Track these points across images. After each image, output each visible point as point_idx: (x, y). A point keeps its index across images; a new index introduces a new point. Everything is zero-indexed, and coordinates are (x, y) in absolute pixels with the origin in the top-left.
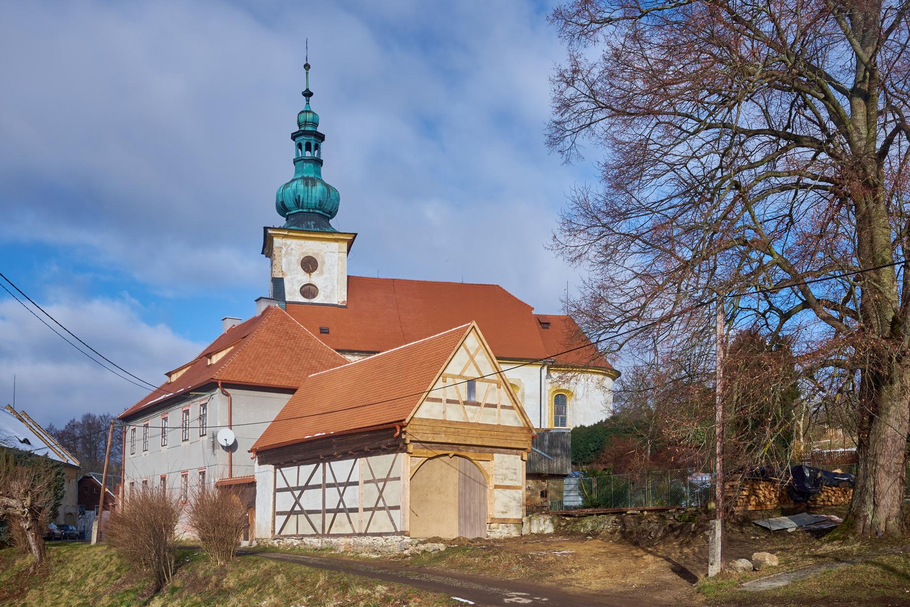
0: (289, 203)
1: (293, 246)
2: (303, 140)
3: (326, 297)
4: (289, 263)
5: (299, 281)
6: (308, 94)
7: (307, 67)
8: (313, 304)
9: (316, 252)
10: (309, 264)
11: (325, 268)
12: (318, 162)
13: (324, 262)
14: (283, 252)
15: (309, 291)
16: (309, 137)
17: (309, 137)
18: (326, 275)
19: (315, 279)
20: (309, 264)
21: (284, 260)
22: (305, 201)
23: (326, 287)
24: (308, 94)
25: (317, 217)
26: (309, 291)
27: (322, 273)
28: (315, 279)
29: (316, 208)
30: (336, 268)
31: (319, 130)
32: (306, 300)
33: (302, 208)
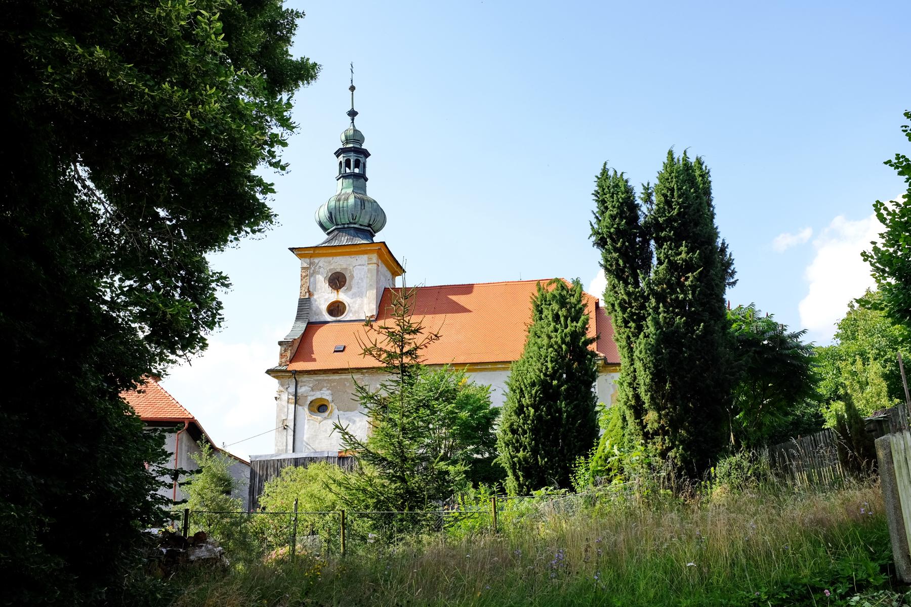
1: (321, 264)
2: (341, 158)
5: (326, 300)
6: (353, 114)
8: (340, 321)
9: (344, 266)
10: (337, 281)
11: (354, 282)
12: (362, 177)
13: (352, 277)
15: (336, 309)
19: (342, 296)
22: (338, 217)
24: (353, 114)
25: (352, 232)
27: (350, 289)
28: (342, 296)
29: (351, 223)
31: (364, 146)
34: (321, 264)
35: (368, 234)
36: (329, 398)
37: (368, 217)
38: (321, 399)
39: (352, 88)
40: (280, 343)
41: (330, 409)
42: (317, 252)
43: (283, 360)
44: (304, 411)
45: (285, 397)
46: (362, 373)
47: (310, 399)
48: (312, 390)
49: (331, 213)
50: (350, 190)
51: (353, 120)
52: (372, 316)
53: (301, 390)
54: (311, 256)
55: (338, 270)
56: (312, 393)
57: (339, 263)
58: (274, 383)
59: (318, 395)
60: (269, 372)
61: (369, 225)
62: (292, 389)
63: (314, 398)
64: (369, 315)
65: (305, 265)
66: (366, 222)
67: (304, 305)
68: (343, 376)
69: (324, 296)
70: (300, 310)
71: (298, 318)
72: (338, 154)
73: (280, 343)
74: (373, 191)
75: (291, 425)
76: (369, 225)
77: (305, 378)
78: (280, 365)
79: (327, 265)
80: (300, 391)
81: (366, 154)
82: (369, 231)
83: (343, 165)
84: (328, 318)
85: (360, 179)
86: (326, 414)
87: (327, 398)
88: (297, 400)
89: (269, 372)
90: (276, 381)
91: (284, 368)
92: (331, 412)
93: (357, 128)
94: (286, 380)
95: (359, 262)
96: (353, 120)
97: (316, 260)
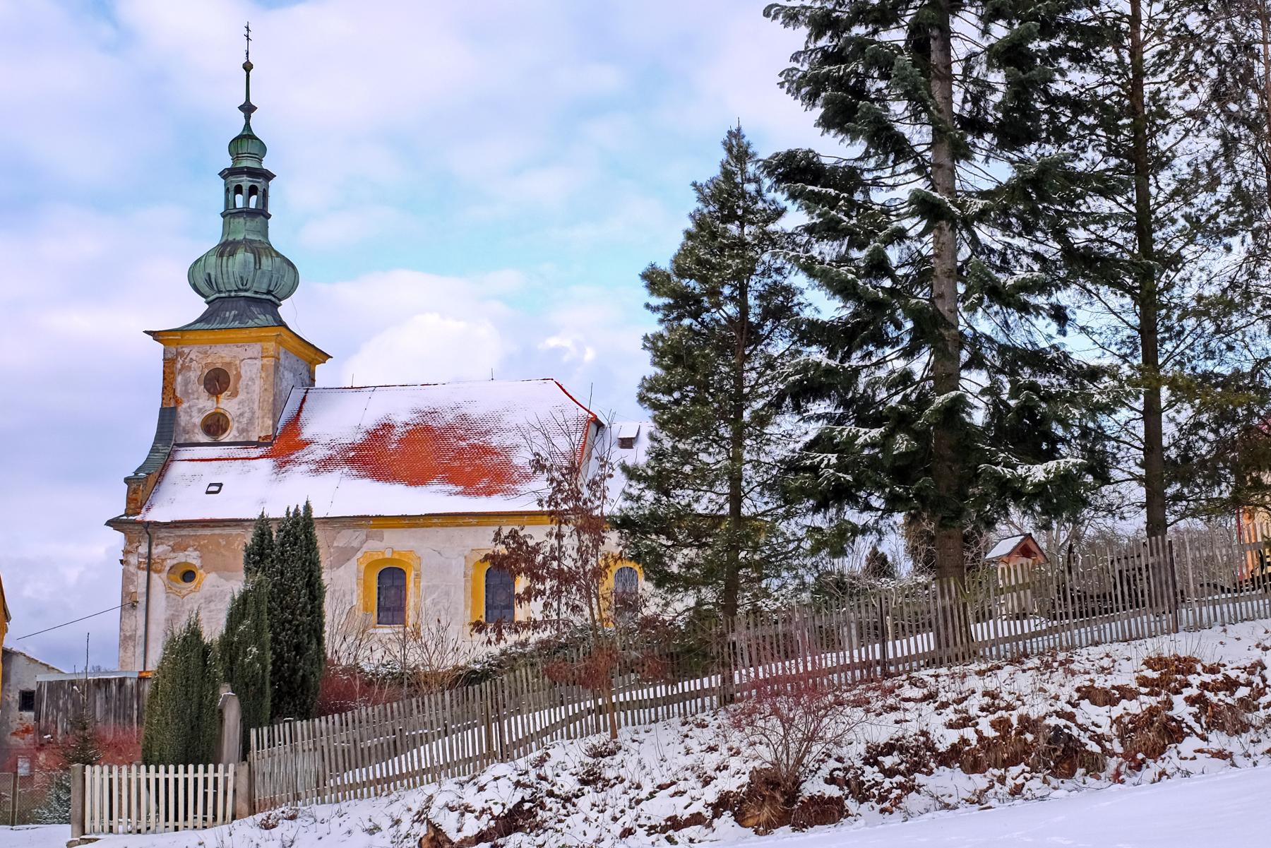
1: (193, 356)
3: (241, 431)
4: (186, 383)
5: (200, 410)
6: (248, 109)
9: (228, 360)
11: (242, 384)
12: (262, 213)
13: (239, 376)
14: (179, 366)
18: (241, 396)
19: (228, 405)
20: (217, 381)
21: (179, 379)
22: (220, 281)
23: (242, 415)
24: (248, 109)
25: (242, 303)
27: (235, 394)
28: (228, 405)
29: (240, 290)
30: (257, 382)
31: (267, 164)
33: (220, 292)
34: (193, 356)
35: (269, 307)
36: (197, 562)
37: (266, 281)
38: (186, 563)
39: (248, 67)
40: (127, 480)
41: (198, 576)
42: (187, 336)
43: (132, 506)
46: (244, 527)
47: (169, 563)
48: (173, 550)
51: (248, 118)
52: (267, 437)
53: (156, 551)
55: (219, 366)
56: (172, 555)
57: (222, 354)
58: (118, 538)
59: (181, 557)
60: (109, 523)
61: (269, 292)
62: (143, 549)
63: (175, 562)
64: (263, 435)
65: (169, 356)
66: (264, 288)
67: (168, 417)
68: (217, 531)
69: (197, 407)
72: (226, 174)
73: (127, 480)
74: (278, 236)
75: (142, 600)
77: (163, 533)
78: (126, 514)
80: (154, 551)
81: (268, 176)
83: (232, 193)
86: (192, 585)
87: (194, 562)
89: (109, 523)
90: (120, 536)
92: (199, 583)
96: (248, 118)
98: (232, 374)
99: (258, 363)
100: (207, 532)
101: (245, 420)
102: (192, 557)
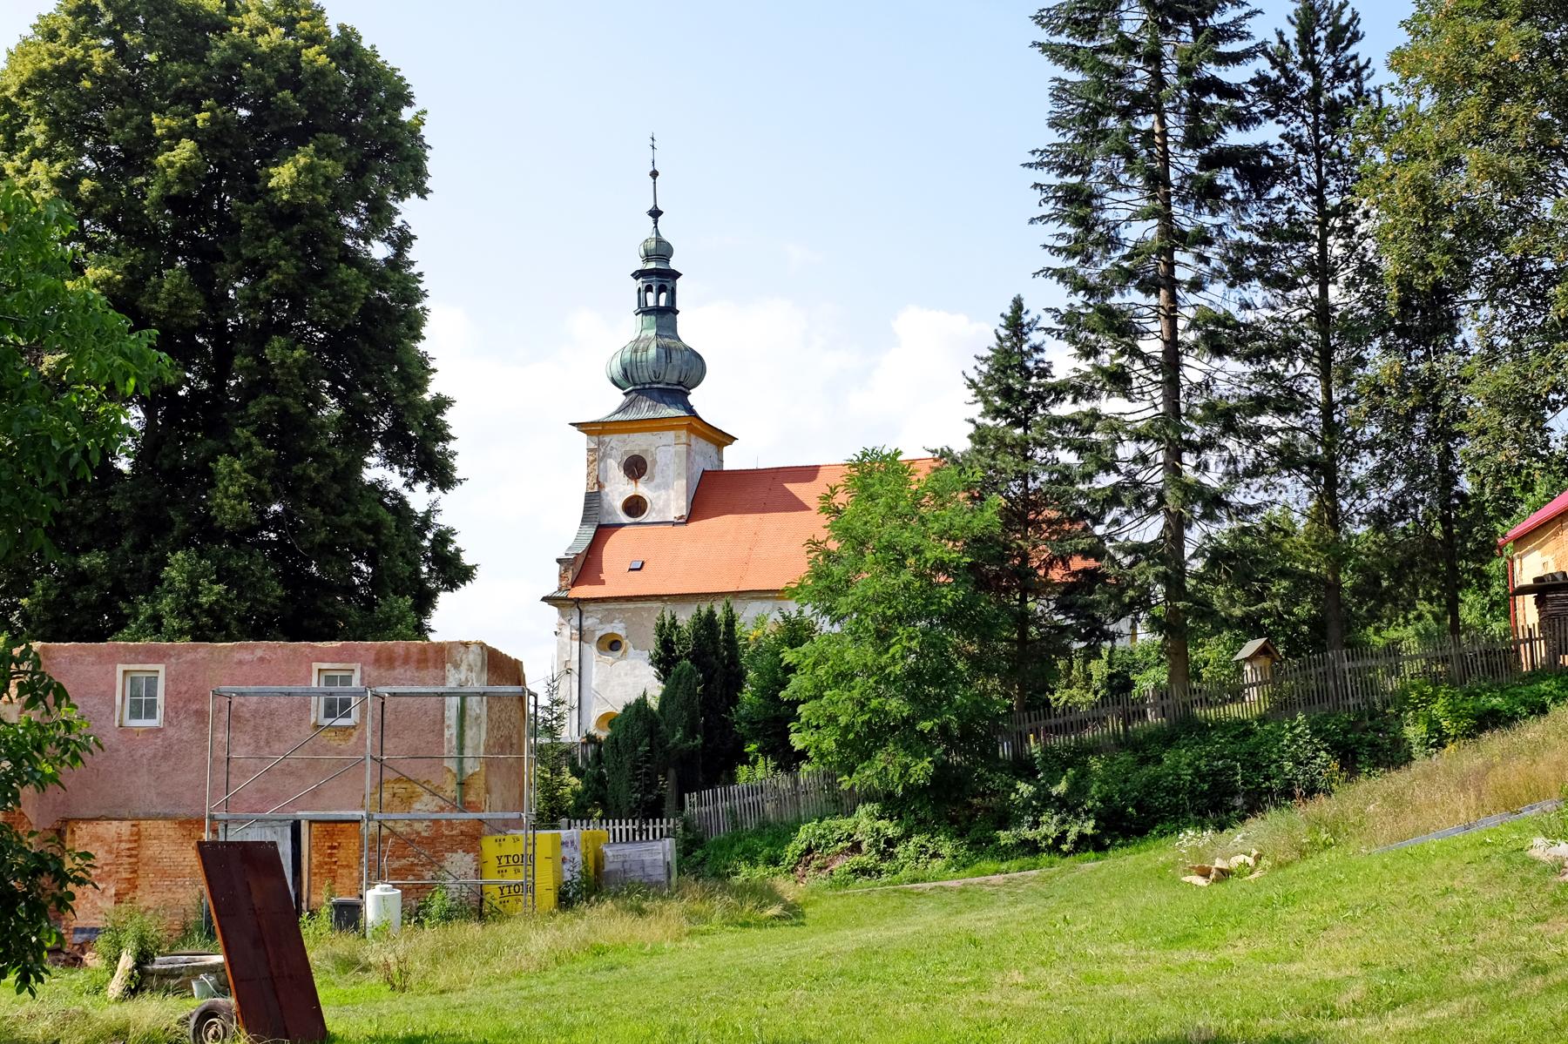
0: (618, 377)
2: (639, 283)
5: (621, 494)
6: (655, 213)
7: (654, 174)
10: (636, 467)
11: (657, 469)
12: (670, 310)
13: (655, 462)
15: (635, 506)
16: (659, 275)
17: (659, 275)
19: (642, 489)
24: (655, 213)
25: (656, 394)
26: (635, 506)
27: (651, 479)
28: (642, 489)
32: (632, 520)
36: (622, 633)
38: (612, 634)
39: (654, 174)
40: (559, 561)
44: (591, 651)
45: (567, 631)
47: (599, 634)
49: (625, 370)
50: (652, 333)
53: (587, 623)
54: (600, 433)
57: (637, 443)
59: (608, 629)
60: (544, 599)
61: (680, 383)
62: (575, 622)
65: (593, 446)
66: (675, 379)
67: (593, 501)
68: (640, 605)
69: (619, 489)
70: (587, 509)
71: (585, 521)
73: (559, 561)
76: (680, 383)
77: (591, 607)
79: (622, 446)
81: (676, 275)
82: (677, 393)
84: (625, 519)
85: (665, 315)
88: (582, 636)
91: (564, 595)
93: (665, 236)
94: (568, 610)
95: (664, 441)
97: (607, 438)
98: (649, 460)
99: (672, 450)
100: (631, 606)
101: (661, 503)
102: (618, 628)
